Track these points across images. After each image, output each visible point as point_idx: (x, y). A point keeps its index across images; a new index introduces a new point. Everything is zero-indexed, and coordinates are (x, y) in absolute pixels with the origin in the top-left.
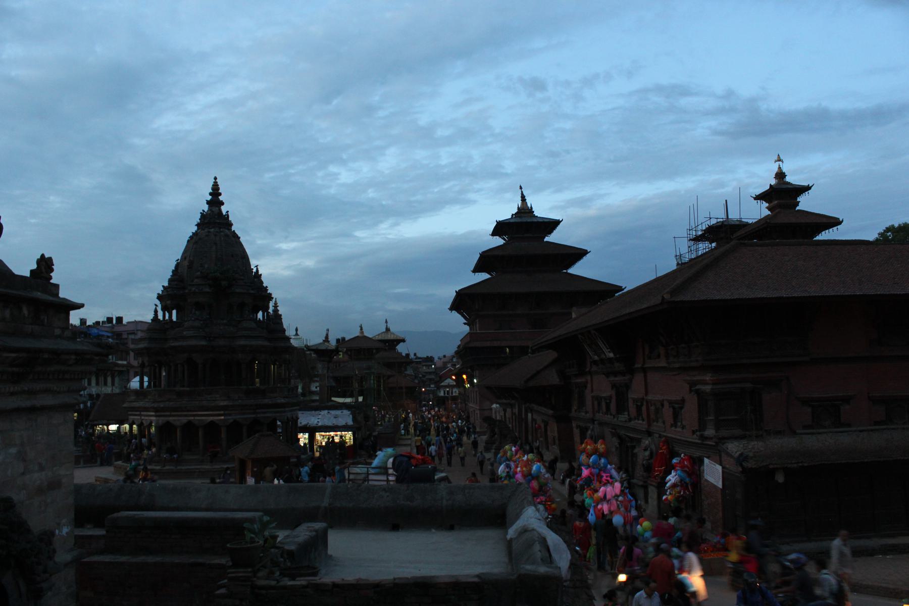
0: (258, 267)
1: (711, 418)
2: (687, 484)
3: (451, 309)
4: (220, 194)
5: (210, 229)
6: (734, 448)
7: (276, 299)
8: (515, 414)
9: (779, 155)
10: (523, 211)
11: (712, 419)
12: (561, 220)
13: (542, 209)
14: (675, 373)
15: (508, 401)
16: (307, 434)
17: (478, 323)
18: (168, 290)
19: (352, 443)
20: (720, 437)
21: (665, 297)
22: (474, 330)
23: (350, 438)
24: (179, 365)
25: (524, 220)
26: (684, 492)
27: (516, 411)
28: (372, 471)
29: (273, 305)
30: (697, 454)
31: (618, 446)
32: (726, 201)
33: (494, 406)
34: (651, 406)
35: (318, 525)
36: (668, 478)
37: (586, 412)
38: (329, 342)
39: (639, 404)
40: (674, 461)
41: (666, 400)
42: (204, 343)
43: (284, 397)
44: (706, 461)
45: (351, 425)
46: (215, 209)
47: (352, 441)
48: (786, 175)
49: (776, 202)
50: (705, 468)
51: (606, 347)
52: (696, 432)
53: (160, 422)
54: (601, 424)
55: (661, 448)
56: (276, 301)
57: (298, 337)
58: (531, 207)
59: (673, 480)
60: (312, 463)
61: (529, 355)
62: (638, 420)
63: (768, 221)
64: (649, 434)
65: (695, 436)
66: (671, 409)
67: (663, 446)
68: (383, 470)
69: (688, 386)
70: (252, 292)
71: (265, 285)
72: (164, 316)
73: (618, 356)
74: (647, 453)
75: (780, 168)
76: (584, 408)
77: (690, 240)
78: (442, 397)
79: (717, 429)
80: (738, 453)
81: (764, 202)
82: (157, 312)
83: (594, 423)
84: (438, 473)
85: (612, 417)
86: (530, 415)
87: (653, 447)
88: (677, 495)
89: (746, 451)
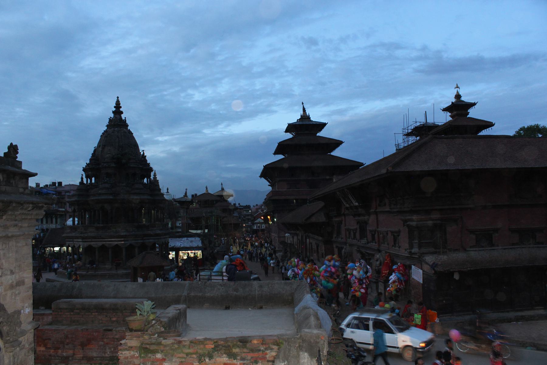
1: (416, 241)
2: (402, 281)
3: (261, 176)
4: (121, 107)
6: (430, 259)
7: (155, 171)
8: (299, 239)
9: (457, 84)
11: (417, 242)
12: (326, 123)
13: (315, 116)
15: (295, 232)
16: (174, 252)
17: (277, 185)
18: (90, 165)
19: (201, 257)
20: (421, 252)
21: (389, 169)
22: (274, 189)
23: (200, 254)
24: (96, 211)
25: (304, 123)
26: (400, 286)
27: (300, 238)
28: (213, 274)
29: (154, 174)
30: (408, 263)
32: (426, 112)
33: (287, 235)
34: (381, 234)
35: (181, 306)
36: (390, 278)
37: (342, 238)
38: (187, 196)
39: (373, 233)
40: (394, 267)
42: (111, 197)
43: (160, 230)
44: (413, 267)
45: (201, 247)
46: (118, 116)
47: (201, 256)
48: (461, 97)
49: (455, 112)
50: (412, 271)
51: (353, 199)
52: (408, 250)
54: (351, 245)
55: (386, 260)
56: (155, 172)
57: (168, 193)
58: (309, 115)
59: (393, 279)
60: (177, 269)
61: (308, 204)
62: (373, 243)
63: (451, 124)
64: (379, 251)
65: (406, 252)
66: (392, 236)
67: (388, 258)
68: (220, 273)
69: (402, 222)
70: (141, 166)
71: (148, 162)
72: (87, 181)
73: (361, 205)
74: (378, 263)
75: (458, 92)
76: (340, 236)
77: (404, 135)
78: (255, 229)
79: (420, 247)
80: (432, 262)
81: (448, 112)
82: (83, 179)
83: (346, 245)
84: (253, 275)
85: (357, 241)
86: (308, 240)
87: (382, 259)
88: (396, 287)
89: (436, 261)
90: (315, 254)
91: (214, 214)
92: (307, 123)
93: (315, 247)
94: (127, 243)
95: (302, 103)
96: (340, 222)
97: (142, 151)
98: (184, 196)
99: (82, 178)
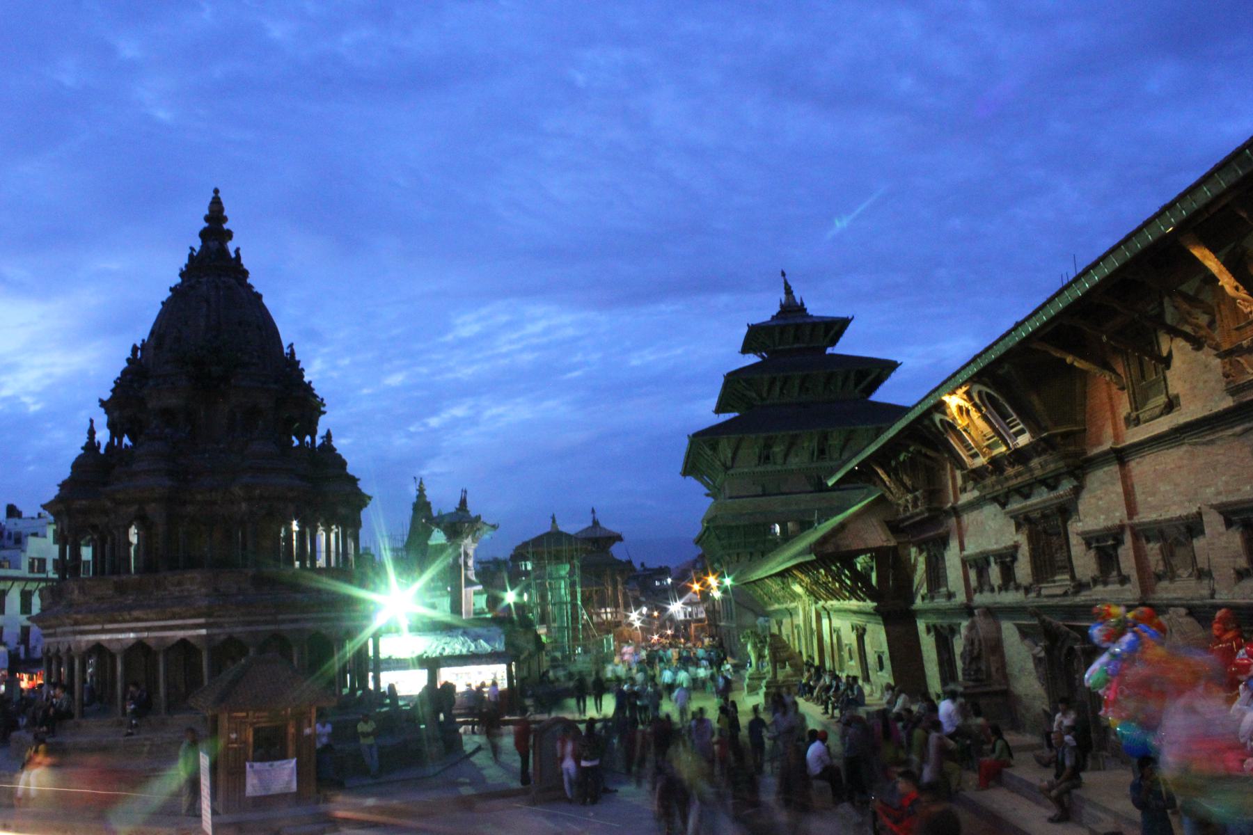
0: (294, 347)
3: (685, 473)
5: (201, 278)
7: (421, 479)
8: (798, 626)
10: (788, 309)
12: (850, 317)
14: (1238, 429)
19: (506, 686)
25: (791, 321)
27: (799, 620)
29: (418, 488)
31: (1042, 654)
33: (761, 620)
34: (1148, 541)
39: (1110, 542)
41: (1212, 506)
46: (213, 245)
53: (83, 644)
54: (993, 612)
56: (421, 483)
58: (802, 304)
61: (816, 525)
62: (1105, 583)
67: (1226, 631)
76: (943, 590)
86: (825, 622)
90: (852, 663)
91: (563, 573)
92: (799, 321)
93: (850, 638)
94: (219, 634)
95: (780, 273)
96: (943, 542)
97: (288, 348)
98: (457, 509)
99: (92, 432)
